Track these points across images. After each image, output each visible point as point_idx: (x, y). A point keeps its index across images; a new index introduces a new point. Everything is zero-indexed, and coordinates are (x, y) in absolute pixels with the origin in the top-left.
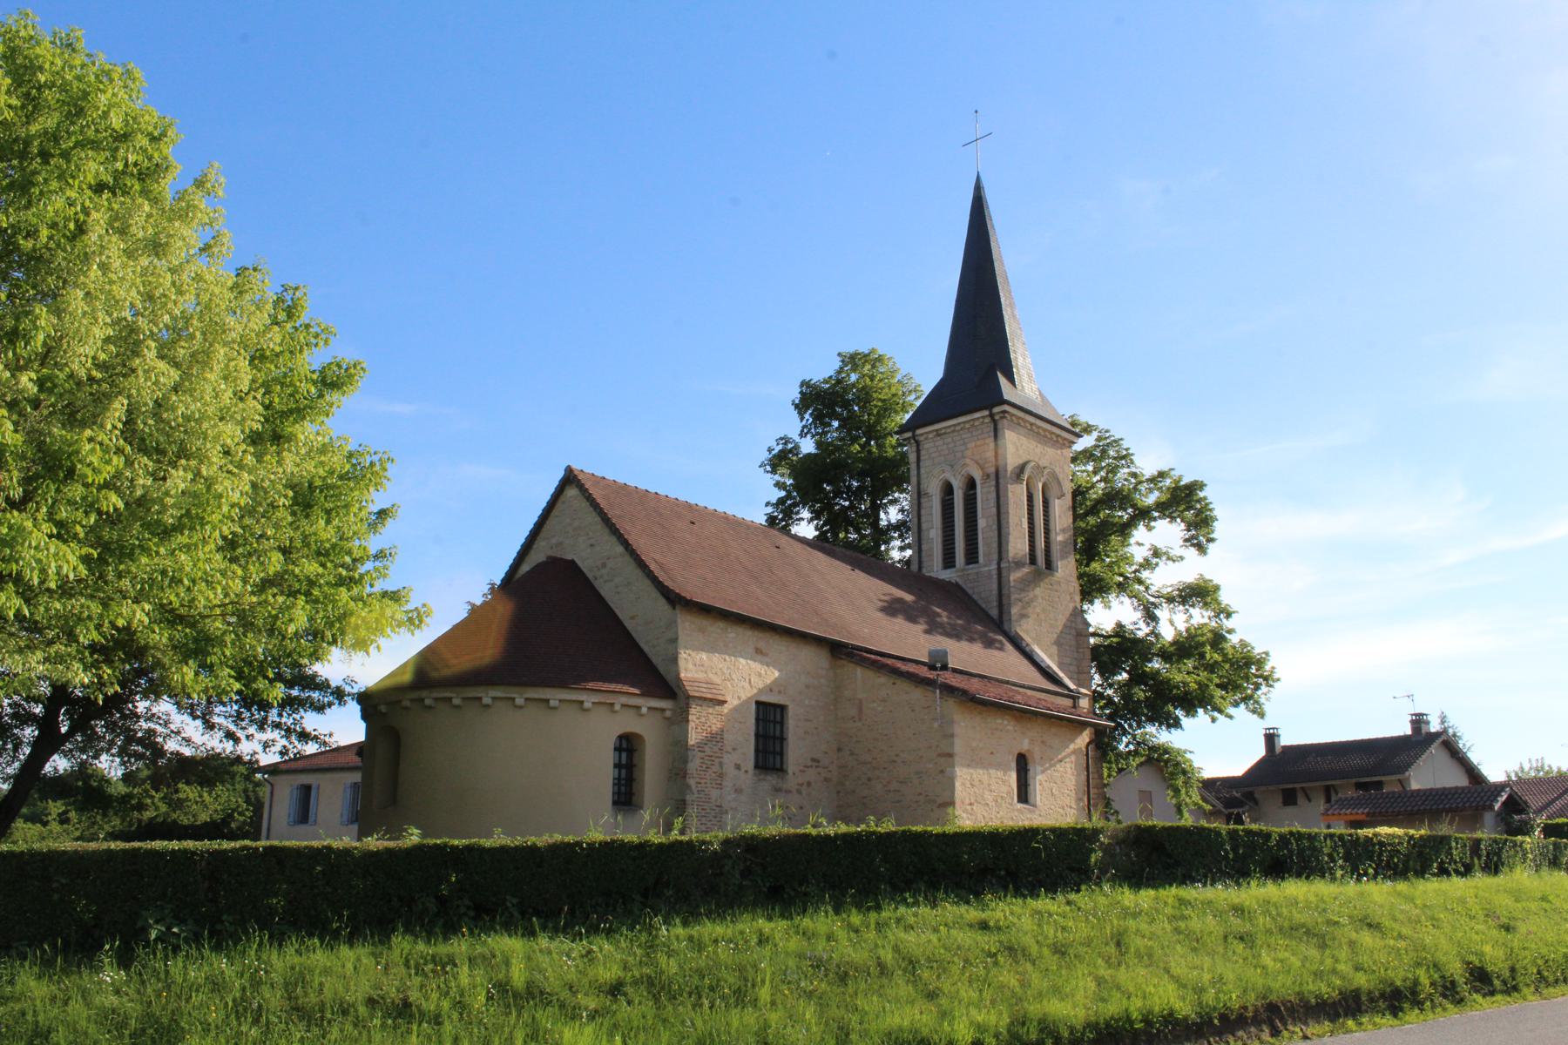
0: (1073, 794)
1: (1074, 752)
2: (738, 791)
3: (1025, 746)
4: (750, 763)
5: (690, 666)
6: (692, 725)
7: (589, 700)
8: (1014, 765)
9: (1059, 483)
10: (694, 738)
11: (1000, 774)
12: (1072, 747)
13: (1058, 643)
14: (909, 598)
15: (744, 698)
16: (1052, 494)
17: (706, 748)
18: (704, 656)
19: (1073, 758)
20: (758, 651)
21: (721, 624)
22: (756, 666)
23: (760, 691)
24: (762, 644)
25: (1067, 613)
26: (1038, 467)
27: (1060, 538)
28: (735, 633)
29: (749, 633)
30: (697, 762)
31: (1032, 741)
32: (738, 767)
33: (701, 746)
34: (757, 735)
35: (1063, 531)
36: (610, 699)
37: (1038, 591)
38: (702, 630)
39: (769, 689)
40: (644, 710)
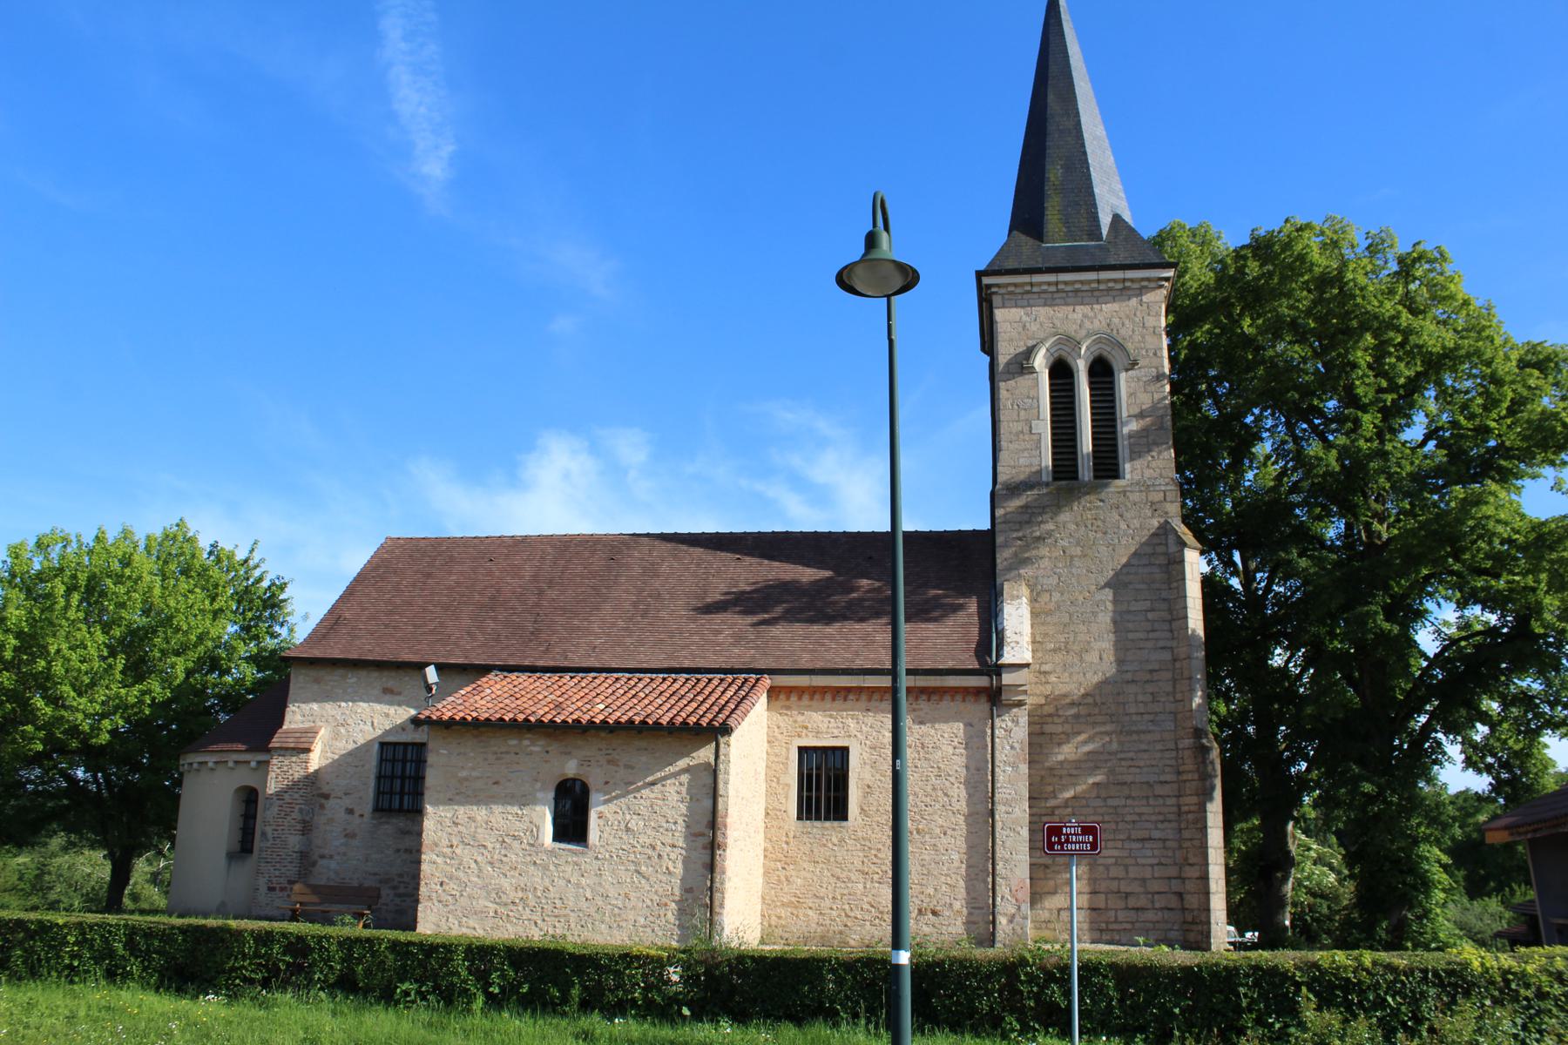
0: (681, 827)
1: (687, 770)
2: (350, 836)
3: (571, 769)
4: (368, 807)
5: (299, 717)
6: (272, 775)
7: (211, 760)
8: (551, 795)
9: (1122, 347)
10: (272, 787)
11: (516, 809)
12: (682, 763)
13: (1117, 584)
14: (828, 574)
15: (361, 741)
16: (1117, 362)
17: (286, 796)
18: (315, 706)
19: (685, 778)
20: (387, 691)
21: (341, 671)
22: (385, 708)
23: (387, 732)
24: (390, 684)
25: (1144, 536)
26: (1069, 338)
27: (1134, 426)
28: (352, 678)
29: (375, 674)
30: (275, 810)
31: (585, 762)
32: (350, 811)
33: (279, 795)
34: (379, 777)
35: (1141, 415)
36: (224, 757)
37: (1065, 516)
38: (317, 681)
39: (402, 728)
40: (231, 764)
